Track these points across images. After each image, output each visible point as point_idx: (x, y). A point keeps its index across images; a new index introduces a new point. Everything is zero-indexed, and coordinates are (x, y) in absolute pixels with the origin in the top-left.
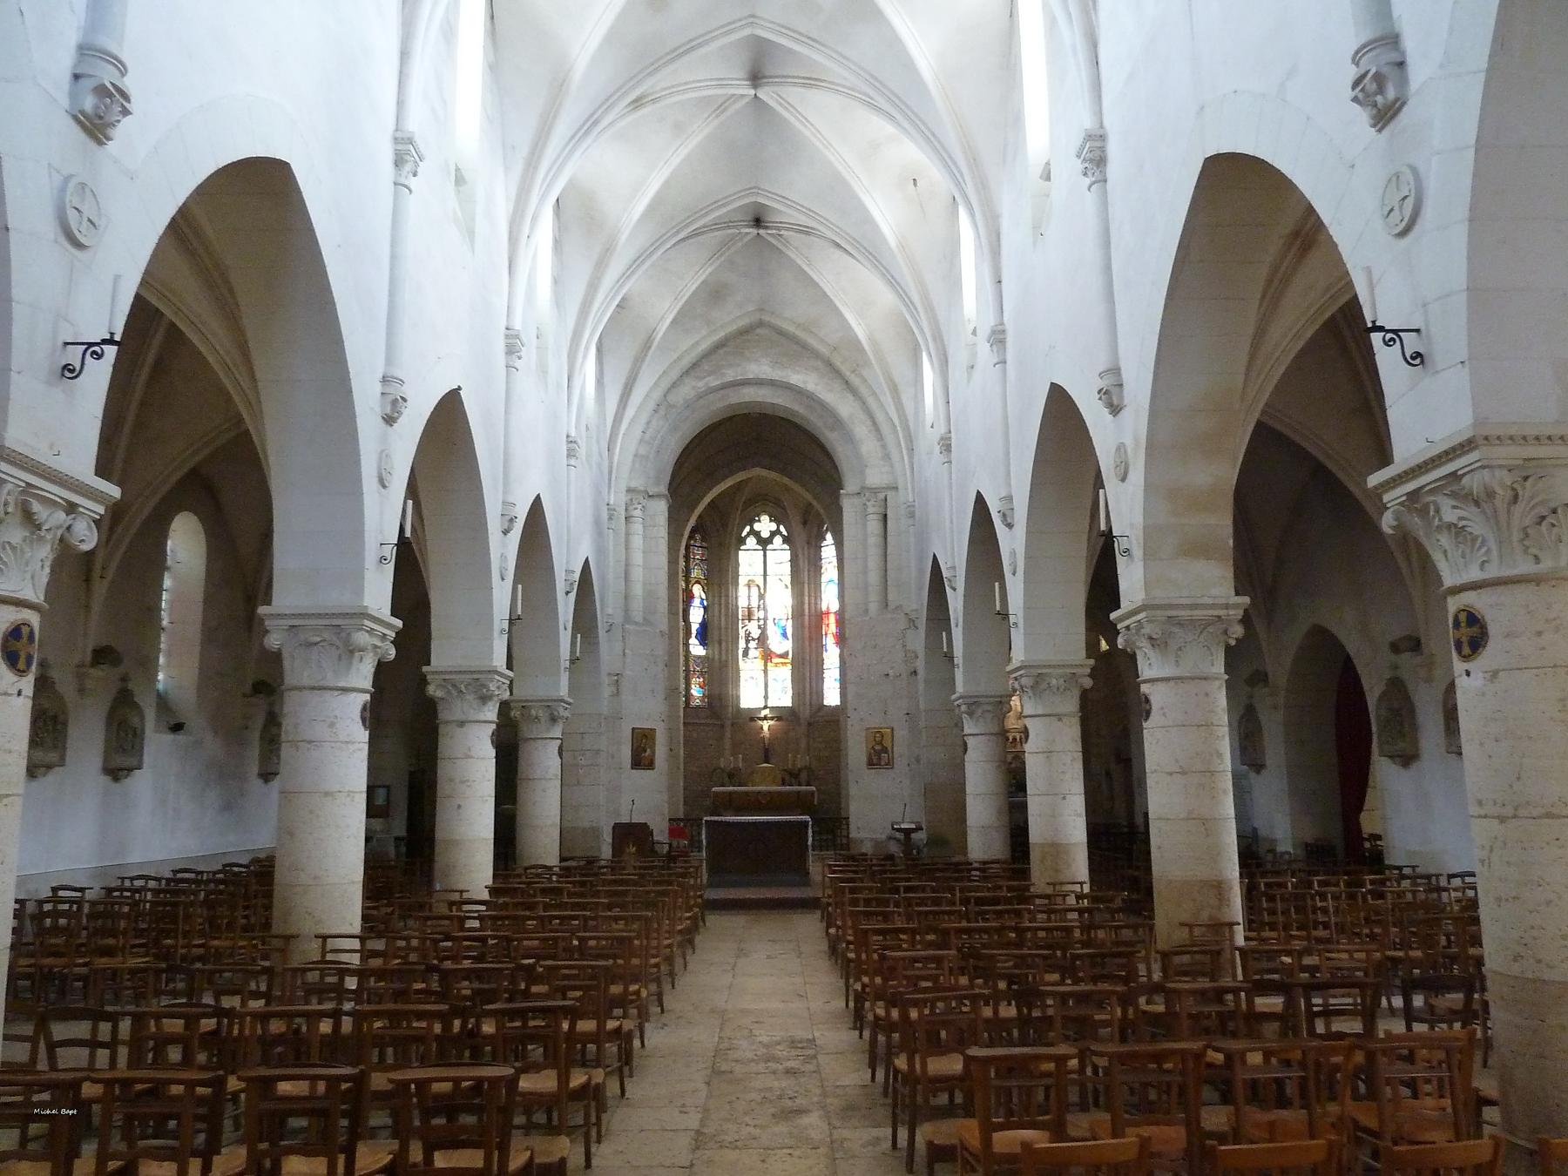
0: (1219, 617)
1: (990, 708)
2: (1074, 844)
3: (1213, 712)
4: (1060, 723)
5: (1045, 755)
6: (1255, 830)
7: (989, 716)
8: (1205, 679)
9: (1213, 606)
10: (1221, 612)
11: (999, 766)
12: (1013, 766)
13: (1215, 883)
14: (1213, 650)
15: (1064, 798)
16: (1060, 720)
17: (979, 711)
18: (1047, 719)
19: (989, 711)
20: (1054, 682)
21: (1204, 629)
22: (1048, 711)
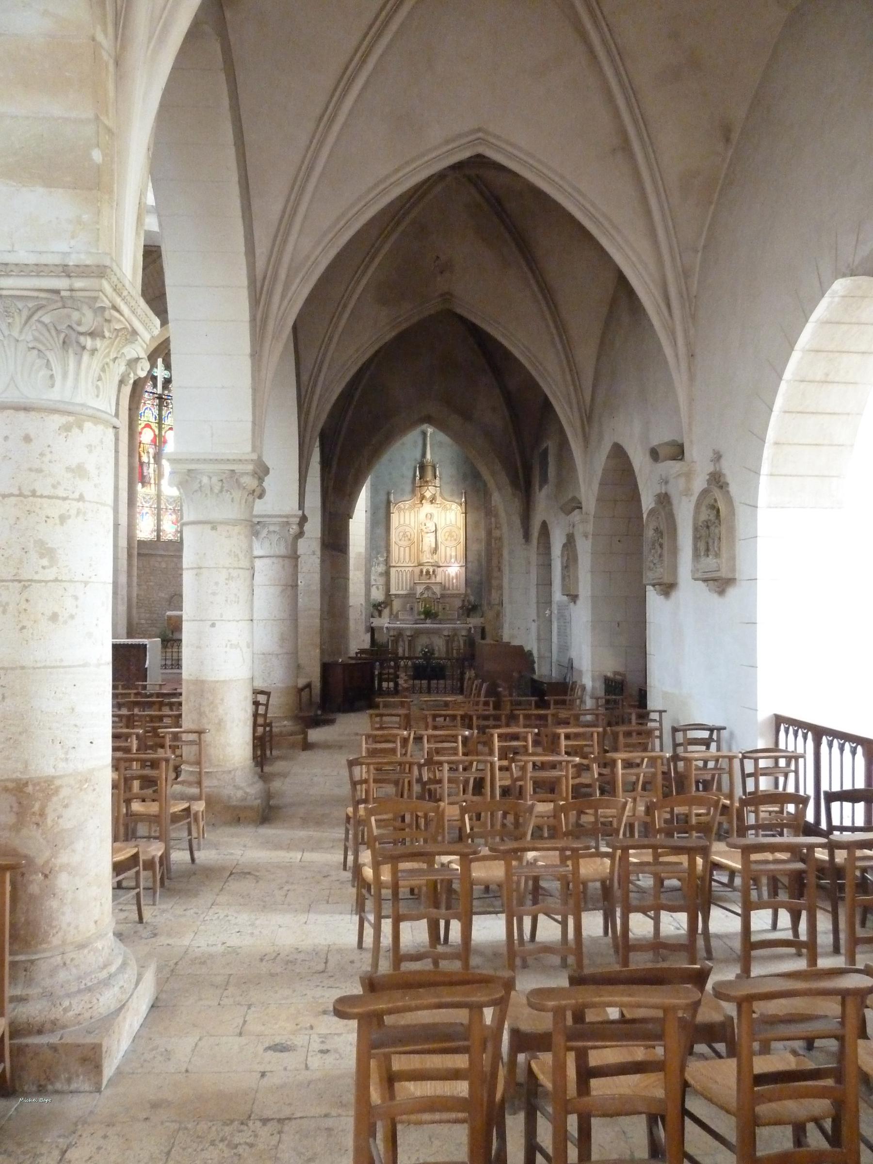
0: (57, 292)
1: (277, 528)
2: (224, 682)
3: (39, 471)
4: (213, 533)
5: (195, 572)
6: (571, 661)
7: (275, 538)
8: (26, 409)
9: (39, 270)
10: (61, 283)
11: (283, 591)
12: (425, 596)
13: (10, 785)
14: (50, 355)
15: (213, 625)
16: (214, 528)
17: (264, 533)
18: (199, 528)
19: (274, 532)
20: (205, 480)
21: (29, 317)
22: (201, 518)
